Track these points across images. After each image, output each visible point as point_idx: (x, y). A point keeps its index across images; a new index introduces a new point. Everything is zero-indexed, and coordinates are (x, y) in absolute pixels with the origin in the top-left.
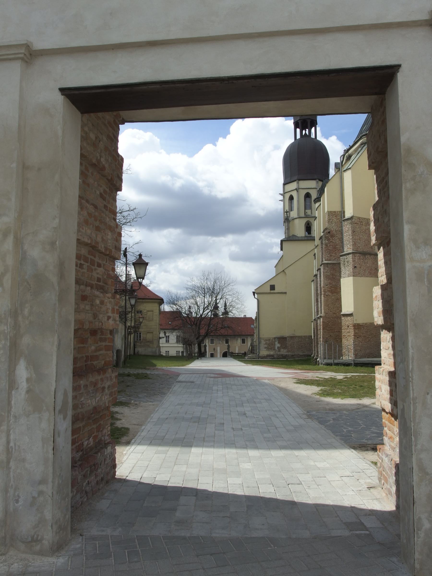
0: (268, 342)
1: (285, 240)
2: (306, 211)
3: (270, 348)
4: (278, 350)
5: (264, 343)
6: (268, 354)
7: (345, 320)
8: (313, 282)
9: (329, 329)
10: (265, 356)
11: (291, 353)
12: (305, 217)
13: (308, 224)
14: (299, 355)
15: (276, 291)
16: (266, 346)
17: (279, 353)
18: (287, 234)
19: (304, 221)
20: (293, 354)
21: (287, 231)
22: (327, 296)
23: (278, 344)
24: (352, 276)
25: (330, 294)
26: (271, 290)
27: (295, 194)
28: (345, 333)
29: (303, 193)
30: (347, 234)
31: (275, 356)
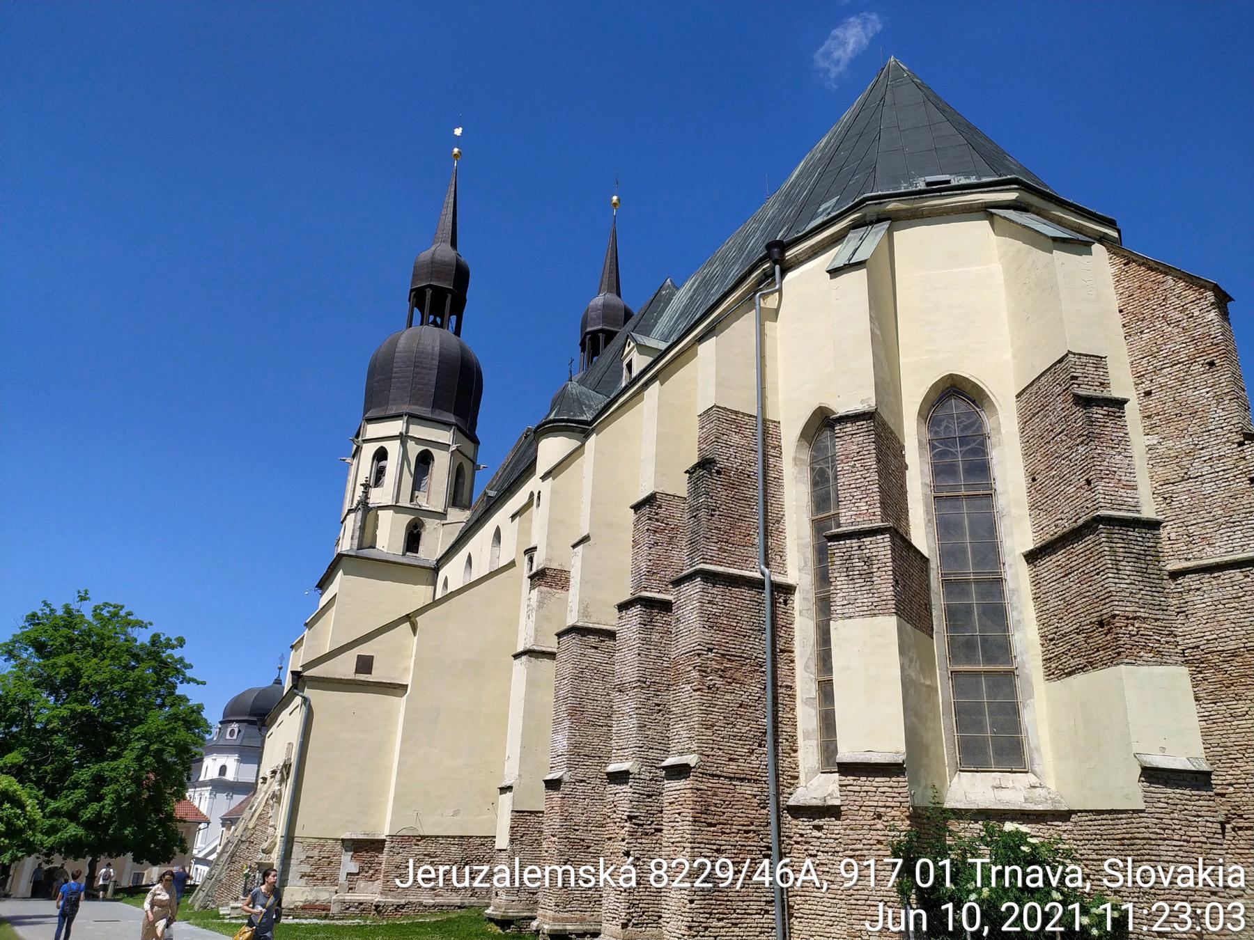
0: (315, 853)
1: (350, 553)
2: (417, 493)
3: (320, 876)
4: (347, 883)
5: (303, 858)
6: (310, 898)
7: (858, 789)
8: (524, 658)
9: (714, 821)
10: (296, 907)
11: (395, 897)
12: (413, 506)
13: (416, 527)
14: (421, 904)
15: (372, 678)
16: (307, 869)
17: (349, 897)
18: (356, 542)
19: (406, 519)
20: (403, 902)
21: (357, 534)
22: (709, 688)
23: (352, 864)
24: (890, 614)
25: (719, 682)
26: (357, 671)
27: (394, 448)
28: (860, 846)
29: (414, 450)
30: (854, 466)
31: (335, 909)
